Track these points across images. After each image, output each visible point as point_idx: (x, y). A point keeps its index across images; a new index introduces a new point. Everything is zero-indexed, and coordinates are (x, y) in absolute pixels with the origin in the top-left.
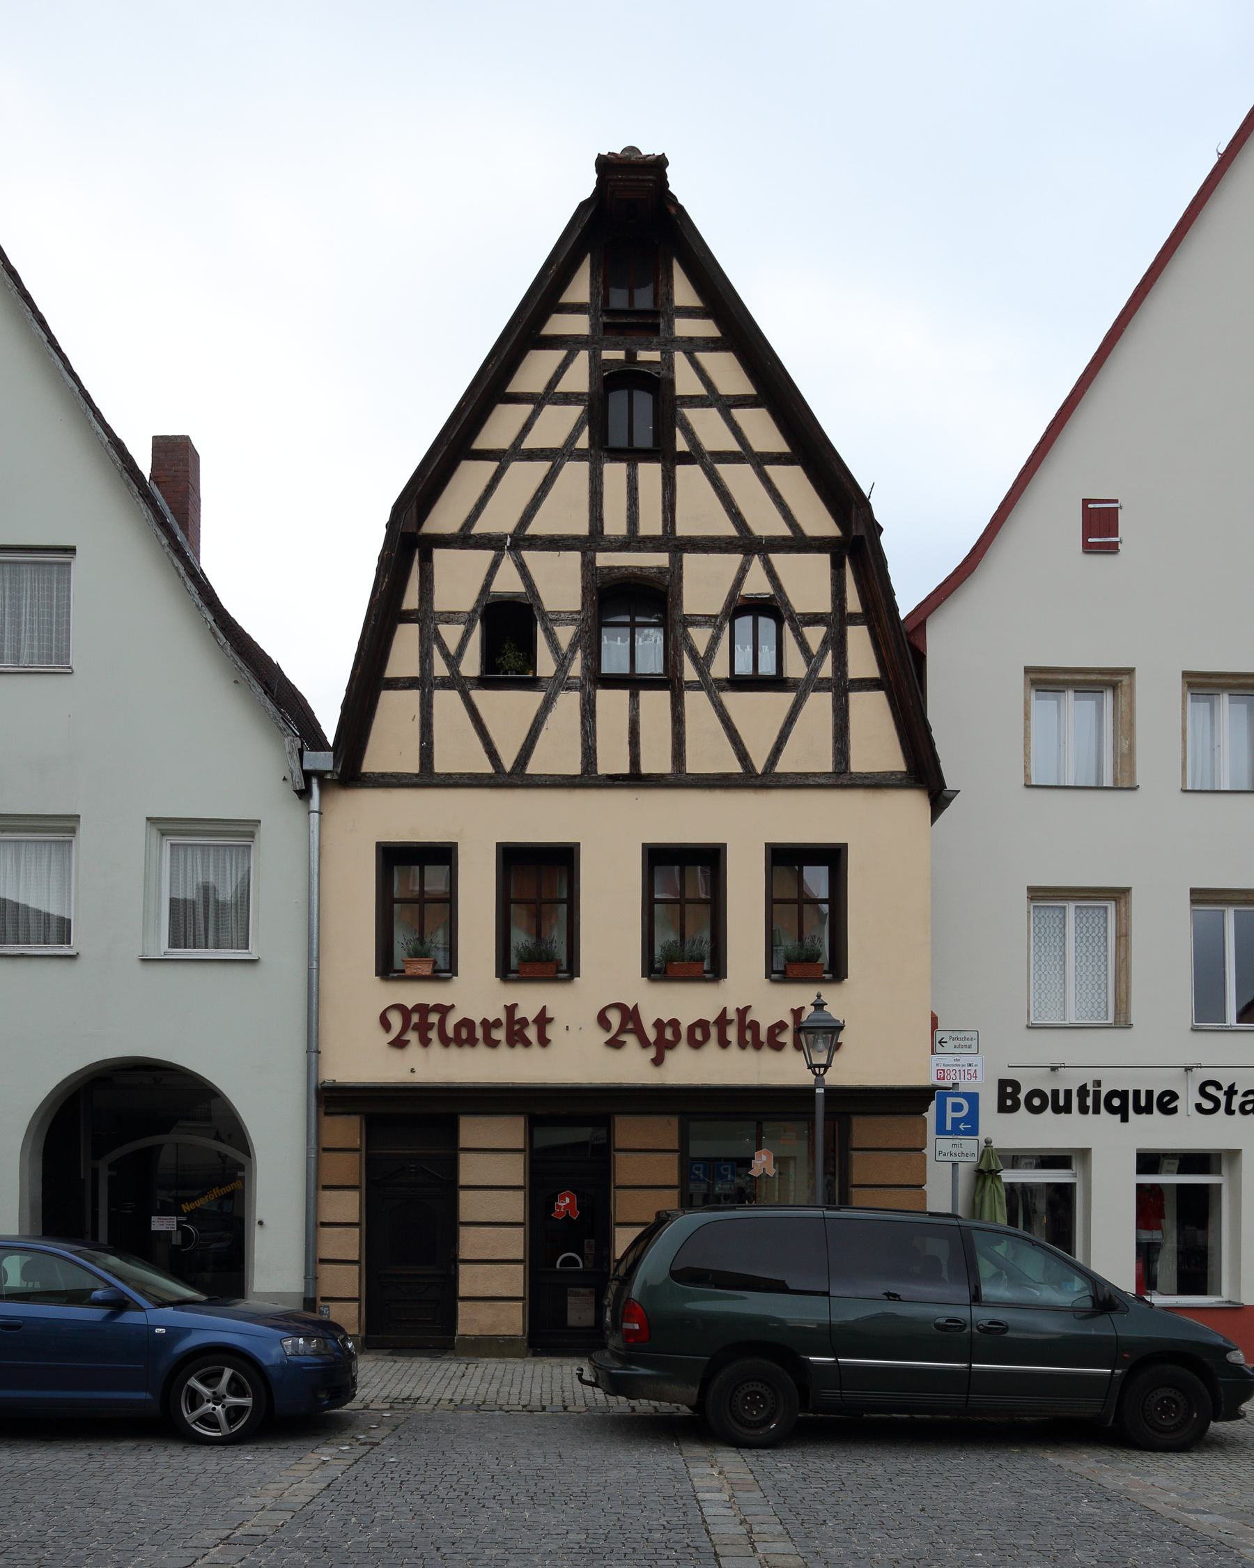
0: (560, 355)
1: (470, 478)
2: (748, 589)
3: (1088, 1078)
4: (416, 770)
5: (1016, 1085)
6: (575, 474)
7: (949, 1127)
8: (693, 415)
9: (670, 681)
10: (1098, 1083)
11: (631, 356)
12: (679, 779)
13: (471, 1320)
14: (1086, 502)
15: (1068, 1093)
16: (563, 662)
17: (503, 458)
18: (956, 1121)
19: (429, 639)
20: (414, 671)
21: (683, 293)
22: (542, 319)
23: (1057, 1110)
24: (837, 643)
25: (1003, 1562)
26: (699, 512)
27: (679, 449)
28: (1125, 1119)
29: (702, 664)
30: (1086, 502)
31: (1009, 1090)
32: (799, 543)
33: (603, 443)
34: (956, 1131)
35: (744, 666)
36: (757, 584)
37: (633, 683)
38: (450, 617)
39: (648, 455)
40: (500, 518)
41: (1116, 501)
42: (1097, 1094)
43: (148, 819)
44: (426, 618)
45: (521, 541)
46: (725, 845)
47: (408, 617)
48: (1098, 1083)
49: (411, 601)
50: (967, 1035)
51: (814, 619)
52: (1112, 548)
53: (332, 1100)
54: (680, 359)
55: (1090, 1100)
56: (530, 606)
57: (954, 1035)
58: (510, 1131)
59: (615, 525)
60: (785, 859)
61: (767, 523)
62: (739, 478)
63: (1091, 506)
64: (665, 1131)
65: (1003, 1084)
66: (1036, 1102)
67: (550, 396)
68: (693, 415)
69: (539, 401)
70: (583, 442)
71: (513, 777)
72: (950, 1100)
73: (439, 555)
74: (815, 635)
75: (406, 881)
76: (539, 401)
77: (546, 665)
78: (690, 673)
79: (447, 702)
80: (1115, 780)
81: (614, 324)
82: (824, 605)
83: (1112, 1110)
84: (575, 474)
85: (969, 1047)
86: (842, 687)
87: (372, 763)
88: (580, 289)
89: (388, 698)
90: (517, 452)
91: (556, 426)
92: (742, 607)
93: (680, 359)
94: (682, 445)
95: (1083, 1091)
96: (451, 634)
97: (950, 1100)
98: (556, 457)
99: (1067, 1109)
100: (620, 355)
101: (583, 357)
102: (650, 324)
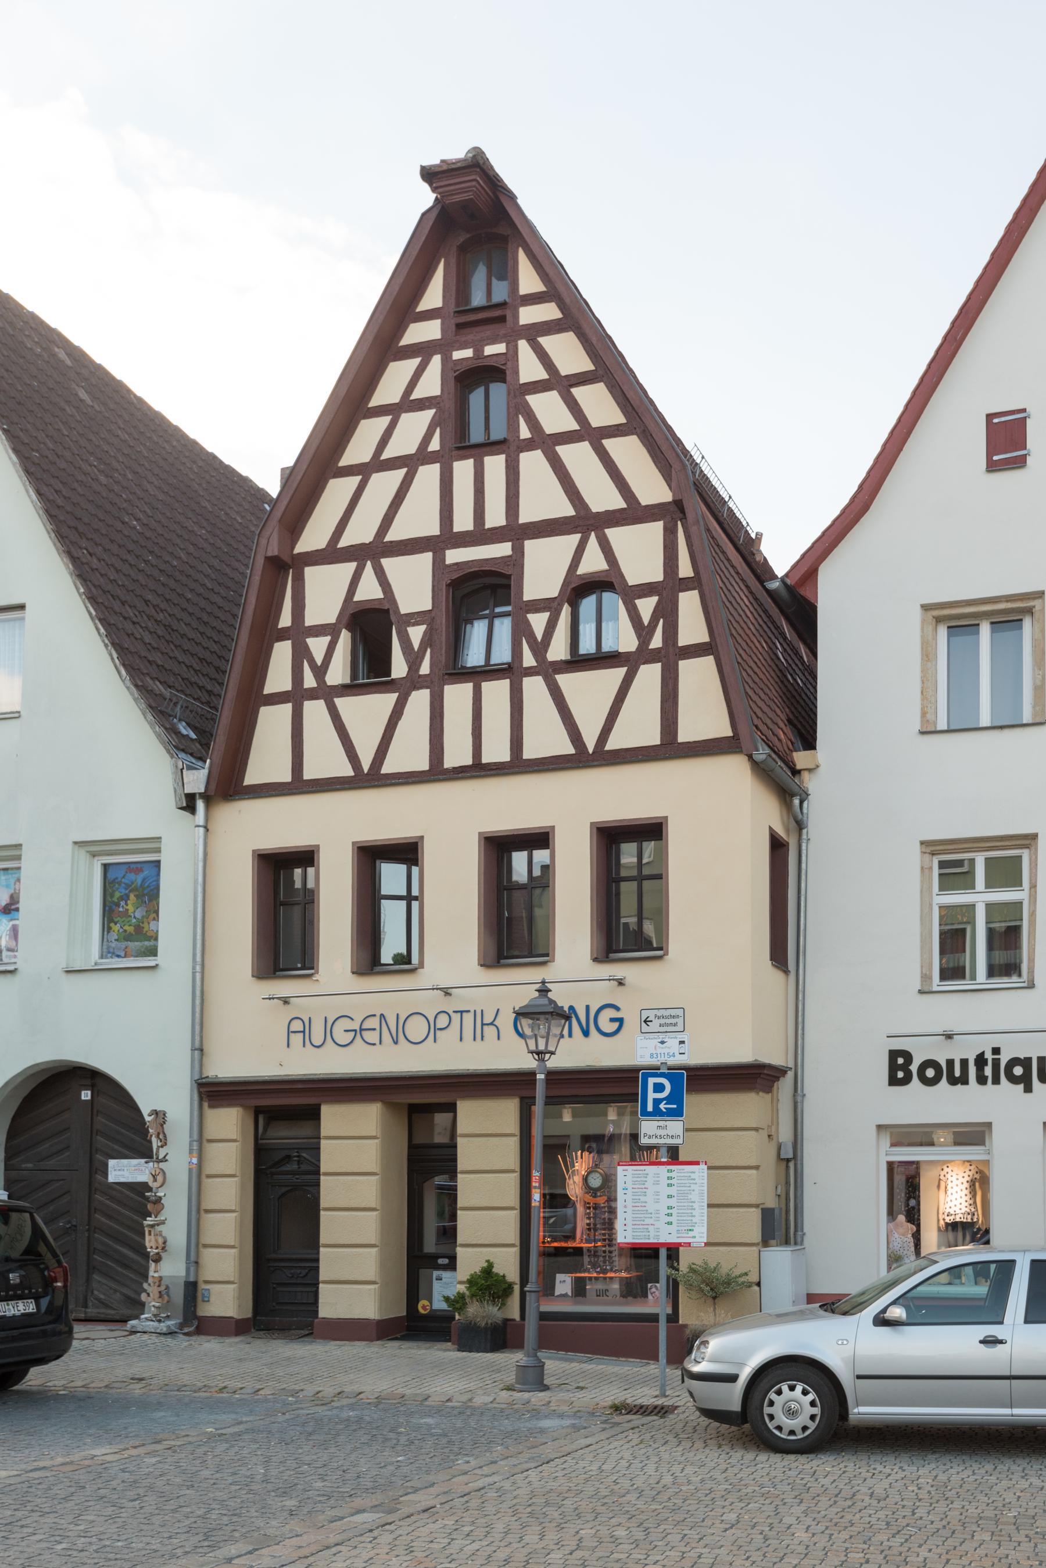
0: (415, 362)
1: (337, 492)
2: (585, 568)
3: (985, 1046)
4: (289, 779)
5: (908, 1056)
6: (429, 475)
7: (650, 1108)
8: (534, 401)
9: (512, 671)
10: (996, 1051)
11: (479, 352)
12: (518, 765)
14: (990, 417)
15: (964, 1063)
16: (413, 660)
17: (364, 471)
18: (657, 1102)
19: (301, 653)
20: (287, 685)
21: (529, 281)
22: (400, 329)
23: (953, 1081)
24: (667, 612)
25: (867, 1562)
26: (541, 499)
27: (522, 437)
28: (1028, 1089)
29: (540, 649)
30: (990, 417)
31: (900, 1061)
32: (634, 513)
33: (460, 440)
34: (657, 1112)
35: (588, 645)
36: (593, 562)
37: (512, 671)
38: (318, 631)
39: (492, 446)
40: (361, 531)
41: (1024, 410)
42: (996, 1063)
43: (75, 843)
44: (299, 633)
45: (376, 551)
46: (592, 824)
47: (283, 635)
48: (996, 1051)
49: (285, 620)
50: (673, 1012)
51: (647, 589)
52: (1020, 463)
54: (523, 345)
55: (987, 1068)
56: (387, 611)
57: (659, 1013)
58: (505, 1113)
59: (463, 521)
60: (610, 837)
61: (602, 497)
62: (578, 457)
63: (996, 421)
64: (505, 1113)
65: (893, 1055)
66: (930, 1073)
67: (409, 404)
68: (534, 401)
69: (395, 411)
70: (435, 445)
71: (369, 778)
72: (651, 1081)
73: (309, 571)
74: (646, 606)
75: (392, 876)
76: (395, 411)
77: (399, 668)
78: (529, 660)
79: (315, 711)
81: (467, 320)
82: (657, 575)
83: (1013, 1079)
84: (429, 475)
85: (675, 1025)
86: (671, 657)
87: (252, 777)
88: (433, 297)
89: (266, 713)
90: (378, 464)
91: (412, 432)
92: (580, 589)
93: (523, 345)
94: (525, 433)
95: (981, 1061)
96: (318, 646)
97: (651, 1081)
98: (411, 463)
99: (964, 1080)
100: (468, 353)
101: (436, 361)
102: (497, 318)
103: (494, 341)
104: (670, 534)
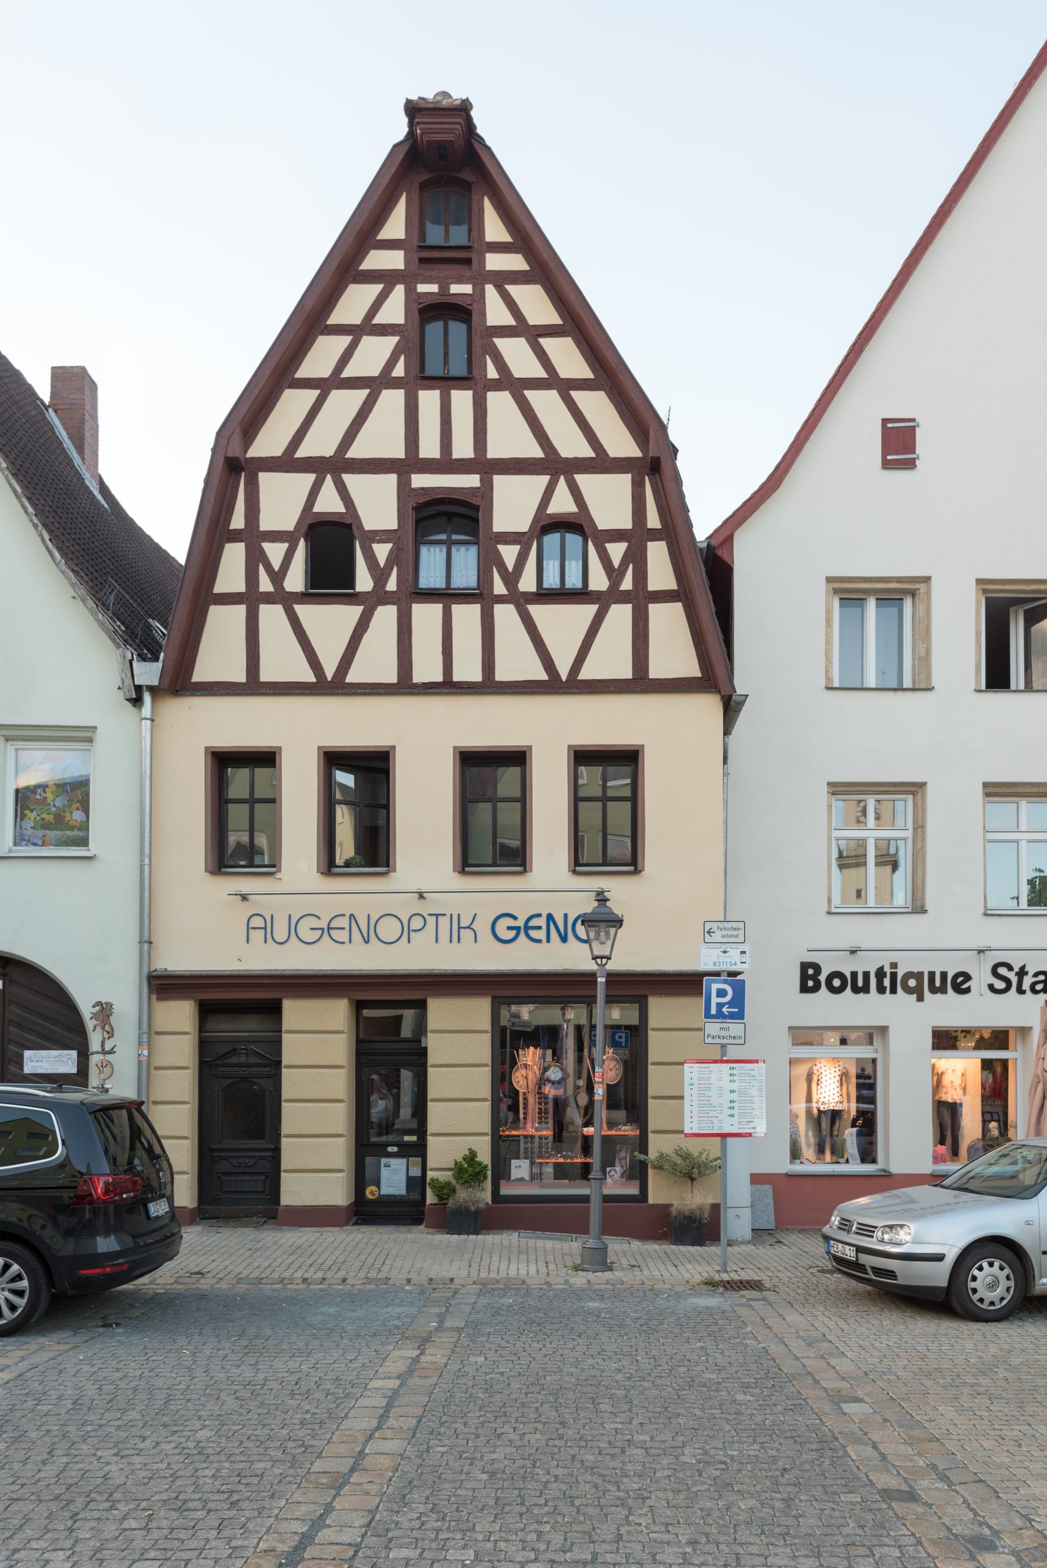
1: (293, 404)
2: (553, 508)
3: (884, 961)
6: (392, 401)
9: (480, 595)
10: (894, 965)
12: (489, 685)
13: (294, 1191)
14: (885, 421)
15: (866, 975)
16: (380, 576)
17: (324, 386)
19: (255, 558)
20: (239, 586)
21: (494, 229)
23: (856, 990)
24: (637, 558)
26: (510, 437)
28: (920, 998)
29: (511, 579)
30: (885, 421)
31: (811, 972)
32: (602, 463)
35: (551, 581)
36: (562, 503)
38: (276, 536)
39: (463, 381)
40: (321, 442)
41: (914, 420)
42: (894, 976)
44: (253, 537)
47: (235, 536)
48: (894, 965)
49: (238, 521)
51: (617, 535)
52: (910, 465)
53: (164, 986)
54: (490, 290)
55: (887, 981)
56: (350, 526)
59: (429, 448)
61: (572, 445)
62: (547, 404)
63: (890, 425)
64: (478, 1011)
65: (804, 966)
66: (837, 983)
67: (368, 327)
70: (399, 371)
71: (333, 685)
74: (617, 551)
77: (364, 582)
78: (499, 588)
79: (272, 616)
80: (914, 682)
81: (427, 258)
82: (626, 523)
83: (908, 990)
84: (392, 401)
86: (642, 599)
87: (201, 674)
88: (395, 227)
90: (337, 381)
91: (373, 355)
92: (547, 524)
93: (490, 290)
94: (492, 373)
95: (880, 973)
96: (275, 552)
98: (375, 385)
99: (866, 989)
100: (434, 288)
101: (399, 290)
102: (464, 258)
103: (460, 281)
104: (637, 488)
